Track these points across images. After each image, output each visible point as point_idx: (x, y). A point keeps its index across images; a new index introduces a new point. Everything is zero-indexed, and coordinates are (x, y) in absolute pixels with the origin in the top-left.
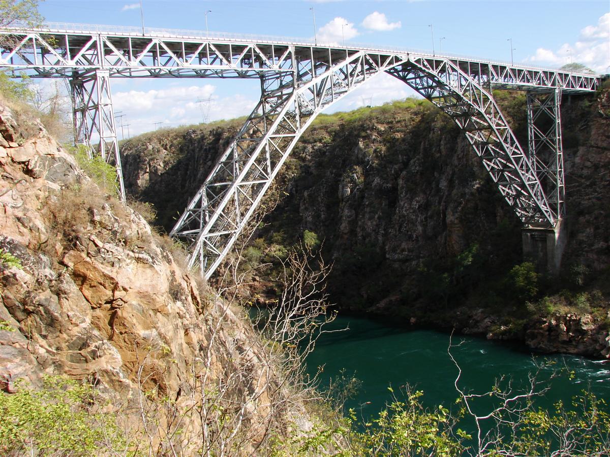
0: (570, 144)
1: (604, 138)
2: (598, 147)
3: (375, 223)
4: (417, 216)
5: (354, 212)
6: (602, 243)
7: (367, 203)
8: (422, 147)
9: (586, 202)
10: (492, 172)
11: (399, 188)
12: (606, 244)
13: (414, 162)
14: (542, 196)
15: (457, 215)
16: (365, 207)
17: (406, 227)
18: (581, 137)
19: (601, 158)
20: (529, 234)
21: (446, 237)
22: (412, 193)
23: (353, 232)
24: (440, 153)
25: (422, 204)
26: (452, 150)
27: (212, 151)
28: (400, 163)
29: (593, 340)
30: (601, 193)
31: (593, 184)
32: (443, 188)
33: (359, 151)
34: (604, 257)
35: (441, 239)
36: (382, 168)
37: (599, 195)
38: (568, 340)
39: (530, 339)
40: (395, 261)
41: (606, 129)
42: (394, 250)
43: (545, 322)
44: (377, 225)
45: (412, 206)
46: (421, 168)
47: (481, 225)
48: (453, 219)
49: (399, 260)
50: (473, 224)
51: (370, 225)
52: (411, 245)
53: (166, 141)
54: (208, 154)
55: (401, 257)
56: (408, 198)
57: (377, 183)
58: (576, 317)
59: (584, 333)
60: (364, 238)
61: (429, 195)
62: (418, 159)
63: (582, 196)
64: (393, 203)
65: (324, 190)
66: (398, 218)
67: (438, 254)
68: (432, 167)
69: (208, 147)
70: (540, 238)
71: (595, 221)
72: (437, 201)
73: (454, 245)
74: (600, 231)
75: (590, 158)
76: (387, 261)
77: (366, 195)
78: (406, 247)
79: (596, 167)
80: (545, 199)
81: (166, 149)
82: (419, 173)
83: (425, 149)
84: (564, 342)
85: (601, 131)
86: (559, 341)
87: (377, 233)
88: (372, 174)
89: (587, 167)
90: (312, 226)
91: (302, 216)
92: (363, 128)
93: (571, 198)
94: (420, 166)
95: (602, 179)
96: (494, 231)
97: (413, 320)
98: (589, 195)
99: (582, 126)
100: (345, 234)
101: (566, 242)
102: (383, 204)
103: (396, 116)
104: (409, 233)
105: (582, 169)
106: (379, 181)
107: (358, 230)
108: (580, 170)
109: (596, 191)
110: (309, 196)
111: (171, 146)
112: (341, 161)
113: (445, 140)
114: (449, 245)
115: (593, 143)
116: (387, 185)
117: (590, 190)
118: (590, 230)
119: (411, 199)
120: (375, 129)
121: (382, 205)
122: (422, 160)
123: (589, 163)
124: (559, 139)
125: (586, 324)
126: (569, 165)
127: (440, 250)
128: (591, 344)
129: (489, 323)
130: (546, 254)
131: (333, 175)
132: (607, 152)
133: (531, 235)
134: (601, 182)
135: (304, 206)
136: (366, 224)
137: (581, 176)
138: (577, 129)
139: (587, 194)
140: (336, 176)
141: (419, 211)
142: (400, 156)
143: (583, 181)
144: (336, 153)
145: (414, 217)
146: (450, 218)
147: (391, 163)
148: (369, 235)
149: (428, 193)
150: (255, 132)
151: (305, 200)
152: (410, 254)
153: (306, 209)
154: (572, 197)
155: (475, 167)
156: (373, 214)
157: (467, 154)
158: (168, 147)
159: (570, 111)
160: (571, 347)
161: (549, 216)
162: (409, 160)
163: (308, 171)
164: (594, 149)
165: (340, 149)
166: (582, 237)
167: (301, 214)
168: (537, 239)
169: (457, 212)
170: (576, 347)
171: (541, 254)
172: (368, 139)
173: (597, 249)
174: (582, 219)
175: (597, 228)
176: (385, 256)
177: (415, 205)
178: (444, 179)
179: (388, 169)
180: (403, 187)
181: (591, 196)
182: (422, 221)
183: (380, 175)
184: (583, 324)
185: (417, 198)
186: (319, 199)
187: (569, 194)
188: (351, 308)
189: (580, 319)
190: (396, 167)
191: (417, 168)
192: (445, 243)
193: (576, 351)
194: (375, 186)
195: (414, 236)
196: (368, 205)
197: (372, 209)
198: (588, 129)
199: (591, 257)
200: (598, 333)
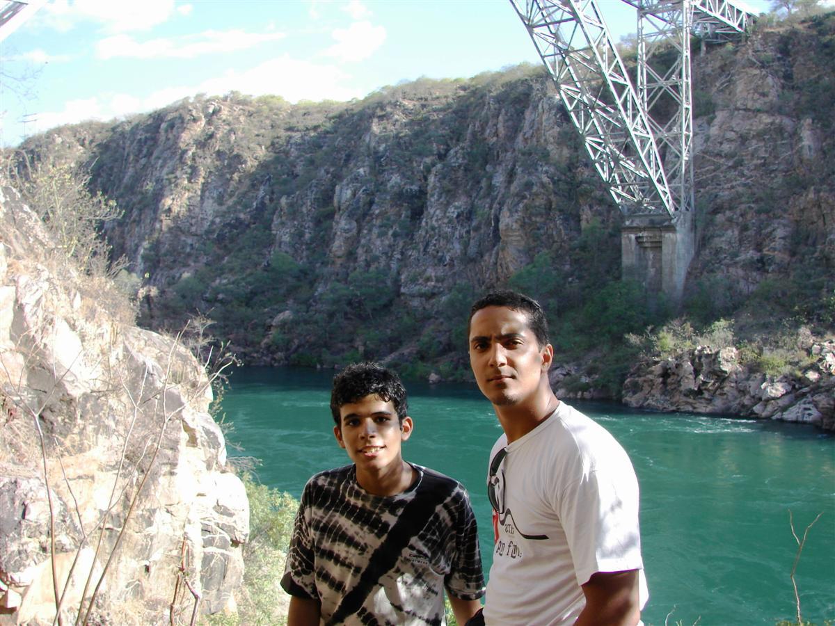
0: (703, 110)
1: (756, 96)
2: (746, 110)
3: (387, 242)
4: (454, 228)
5: (355, 224)
6: (751, 252)
7: (377, 212)
8: (469, 131)
9: (727, 193)
10: (575, 112)
11: (429, 188)
12: (759, 254)
13: (456, 152)
14: (657, 165)
15: (516, 216)
16: (373, 219)
17: (435, 245)
18: (719, 99)
19: (751, 125)
20: (633, 236)
21: (497, 254)
22: (449, 194)
23: (351, 255)
24: (497, 136)
25: (463, 212)
26: (515, 130)
27: (150, 143)
28: (433, 155)
29: (740, 391)
30: (751, 177)
31: (740, 163)
32: (498, 184)
33: (372, 138)
34: (755, 274)
35: (489, 259)
36: (406, 161)
37: (749, 181)
38: (696, 389)
39: (630, 394)
40: (413, 296)
41: (760, 82)
42: (414, 280)
43: (656, 363)
44: (390, 246)
45: (448, 214)
46: (466, 161)
47: (554, 233)
48: (510, 224)
49: (421, 295)
50: (542, 231)
51: (379, 245)
52: (440, 271)
53: (84, 134)
54: (142, 147)
55: (424, 290)
56: (442, 203)
57: (396, 183)
58: (711, 350)
59: (721, 377)
60: (368, 265)
61: (476, 198)
62: (463, 148)
63: (720, 185)
64: (417, 213)
65: (313, 196)
66: (424, 233)
67: (483, 283)
68: (484, 157)
69: (143, 137)
70: (652, 242)
71: (741, 219)
72: (487, 206)
73: (510, 265)
74: (749, 233)
75: (734, 126)
76: (402, 298)
77: (377, 200)
78: (433, 274)
79: (744, 139)
80: (661, 170)
81: (83, 145)
82: (462, 168)
83: (474, 134)
84: (690, 393)
85: (753, 86)
86: (681, 392)
87: (390, 258)
88: (387, 170)
89: (730, 141)
90: (288, 250)
91: (275, 235)
92: (381, 106)
93: (702, 190)
94: (464, 158)
95: (753, 155)
96: (576, 242)
97: (433, 377)
98: (731, 181)
99: (722, 84)
100: (339, 257)
101: (693, 252)
102: (403, 216)
103: (432, 91)
104: (440, 254)
105: (721, 143)
106: (399, 181)
107: (360, 251)
108: (719, 145)
109: (743, 175)
110: (291, 205)
111: (92, 142)
112: (344, 156)
113: (506, 114)
114: (501, 265)
115: (739, 104)
116: (412, 187)
117: (733, 174)
118: (733, 234)
119: (448, 204)
120: (400, 106)
121: (400, 216)
122: (469, 150)
123: (733, 133)
124: (687, 84)
125: (727, 361)
126: (699, 140)
127: (487, 275)
128: (736, 398)
129: (561, 376)
130: (659, 271)
131: (329, 175)
132: (761, 115)
133: (637, 238)
134: (752, 160)
135: (279, 220)
136: (374, 244)
137: (719, 155)
138: (714, 89)
139: (729, 181)
140: (334, 177)
141: (458, 222)
142: (434, 145)
143: (722, 161)
144: (336, 143)
145: (449, 230)
146: (506, 220)
147: (420, 154)
148: (376, 259)
149: (474, 195)
150: (215, 112)
151: (281, 210)
152: (440, 285)
153: (283, 224)
154: (704, 188)
155: (550, 145)
156: (385, 229)
157: (538, 129)
158: (87, 142)
159: (703, 65)
160: (701, 403)
161: (668, 201)
162: (447, 151)
163: (293, 171)
164: (741, 111)
165: (344, 138)
166: (720, 242)
167: (274, 232)
168: (646, 245)
169: (517, 211)
170: (709, 401)
171: (652, 271)
172: (388, 120)
173: (744, 261)
174: (720, 218)
175: (745, 228)
176: (399, 290)
177: (452, 212)
178: (500, 171)
179: (415, 164)
180: (434, 188)
181: (734, 183)
182: (461, 237)
183: (401, 171)
184: (723, 362)
185: (456, 203)
186: (304, 210)
187: (699, 185)
188: (336, 366)
189: (717, 353)
190: (428, 160)
191: (460, 161)
192: (496, 264)
193: (709, 409)
194: (393, 187)
195: (448, 258)
196: (378, 216)
197: (385, 221)
198: (732, 87)
199: (734, 273)
200: (748, 379)
